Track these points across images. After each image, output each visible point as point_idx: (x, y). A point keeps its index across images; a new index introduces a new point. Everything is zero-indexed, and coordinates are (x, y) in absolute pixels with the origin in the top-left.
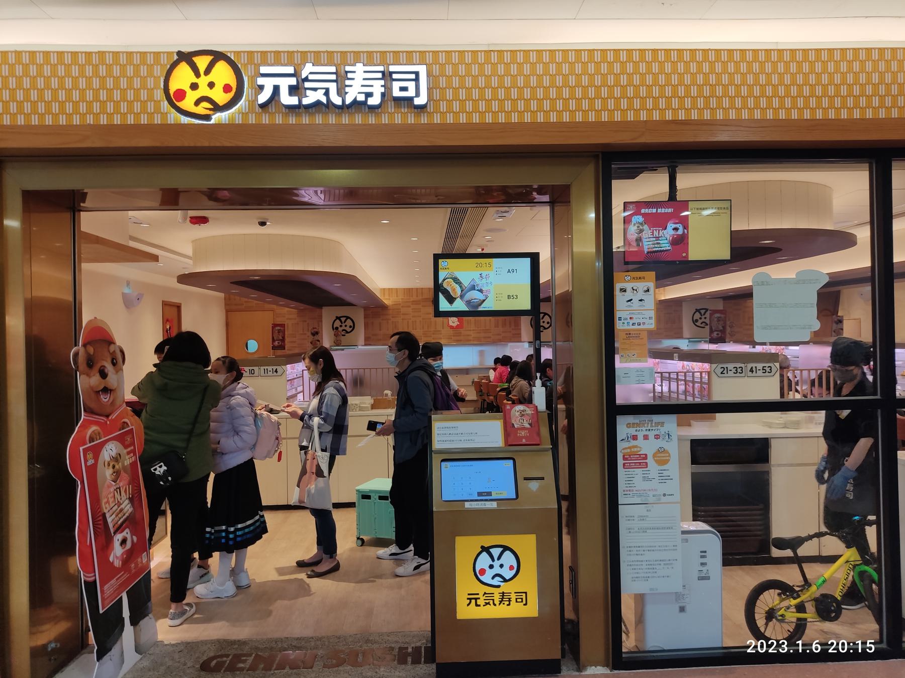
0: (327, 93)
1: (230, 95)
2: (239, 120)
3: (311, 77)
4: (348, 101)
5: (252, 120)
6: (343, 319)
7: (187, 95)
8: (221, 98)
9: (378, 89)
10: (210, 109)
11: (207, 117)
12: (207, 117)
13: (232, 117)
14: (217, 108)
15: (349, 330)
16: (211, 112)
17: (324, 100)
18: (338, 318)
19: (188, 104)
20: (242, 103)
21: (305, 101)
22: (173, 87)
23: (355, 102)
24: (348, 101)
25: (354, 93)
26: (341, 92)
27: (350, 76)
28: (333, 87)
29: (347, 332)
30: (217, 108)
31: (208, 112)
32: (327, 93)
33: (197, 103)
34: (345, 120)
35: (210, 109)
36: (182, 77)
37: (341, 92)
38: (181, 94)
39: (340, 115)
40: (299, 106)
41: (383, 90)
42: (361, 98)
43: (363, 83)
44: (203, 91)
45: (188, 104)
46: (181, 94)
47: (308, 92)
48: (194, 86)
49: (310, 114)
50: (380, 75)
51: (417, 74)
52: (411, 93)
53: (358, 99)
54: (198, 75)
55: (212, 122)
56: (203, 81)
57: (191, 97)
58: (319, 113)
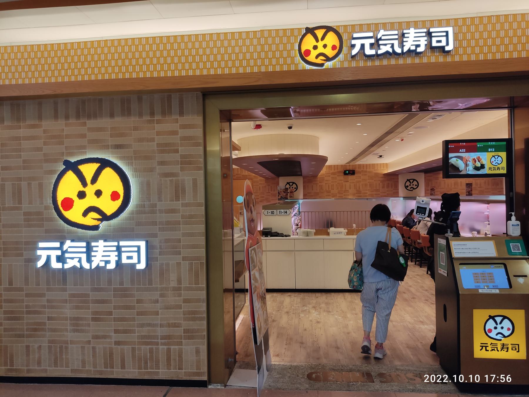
0: (80, 261)
1: (336, 51)
2: (338, 66)
3: (69, 250)
4: (405, 51)
5: (346, 65)
6: (411, 181)
7: (311, 53)
8: (330, 53)
9: (423, 42)
10: (324, 60)
11: (322, 65)
12: (322, 65)
13: (335, 64)
14: (328, 59)
15: (415, 187)
16: (323, 62)
17: (78, 265)
18: (408, 180)
19: (312, 58)
20: (341, 56)
21: (380, 52)
22: (303, 49)
23: (409, 51)
24: (405, 50)
25: (97, 261)
26: (89, 260)
27: (94, 249)
28: (84, 257)
29: (414, 189)
30: (328, 59)
31: (323, 62)
32: (80, 261)
33: (317, 57)
34: (401, 61)
35: (324, 60)
36: (309, 42)
37: (89, 260)
38: (308, 52)
39: (398, 59)
40: (377, 55)
41: (117, 258)
42: (102, 264)
43: (415, 39)
44: (321, 50)
45: (312, 58)
46: (308, 52)
47: (68, 260)
48: (315, 47)
49: (380, 59)
50: (115, 249)
51: (139, 247)
52: (135, 260)
53: (100, 265)
54: (317, 41)
55: (324, 67)
56: (320, 44)
57: (314, 53)
58: (385, 58)
